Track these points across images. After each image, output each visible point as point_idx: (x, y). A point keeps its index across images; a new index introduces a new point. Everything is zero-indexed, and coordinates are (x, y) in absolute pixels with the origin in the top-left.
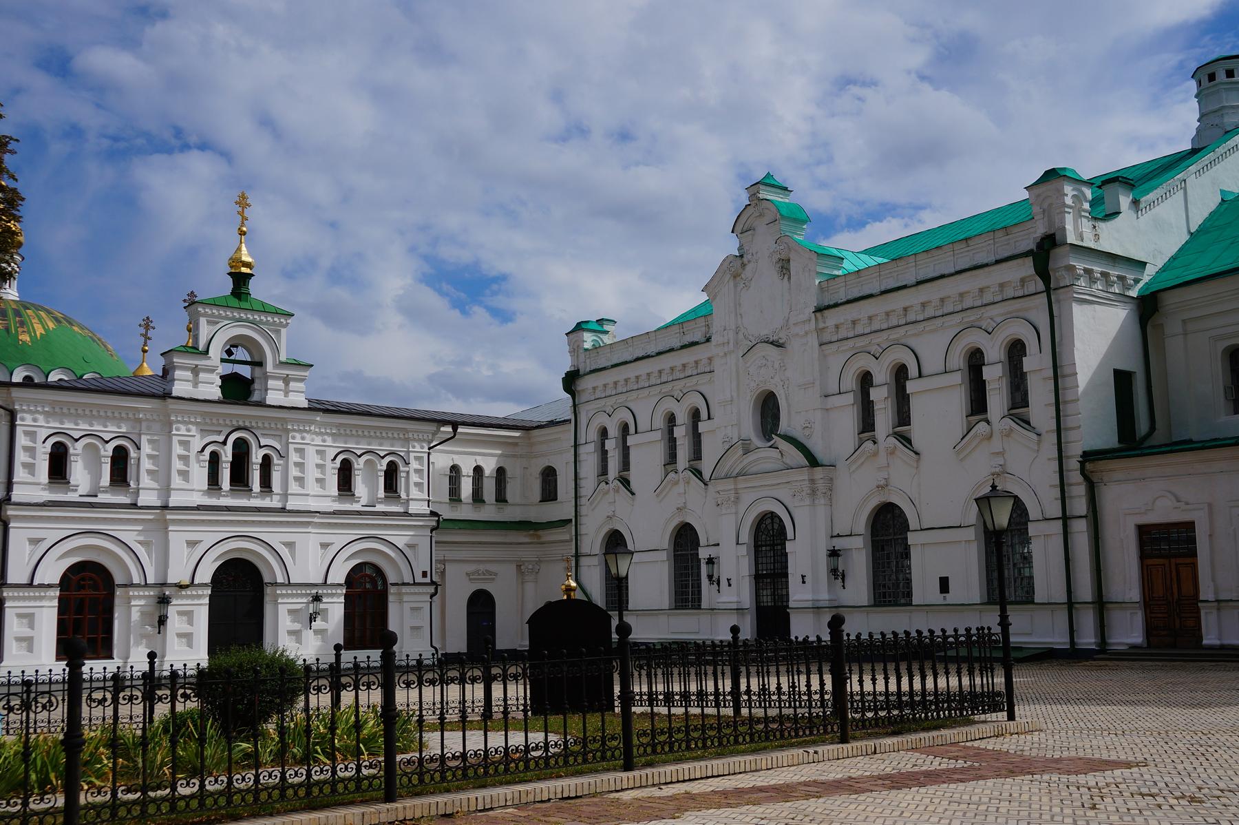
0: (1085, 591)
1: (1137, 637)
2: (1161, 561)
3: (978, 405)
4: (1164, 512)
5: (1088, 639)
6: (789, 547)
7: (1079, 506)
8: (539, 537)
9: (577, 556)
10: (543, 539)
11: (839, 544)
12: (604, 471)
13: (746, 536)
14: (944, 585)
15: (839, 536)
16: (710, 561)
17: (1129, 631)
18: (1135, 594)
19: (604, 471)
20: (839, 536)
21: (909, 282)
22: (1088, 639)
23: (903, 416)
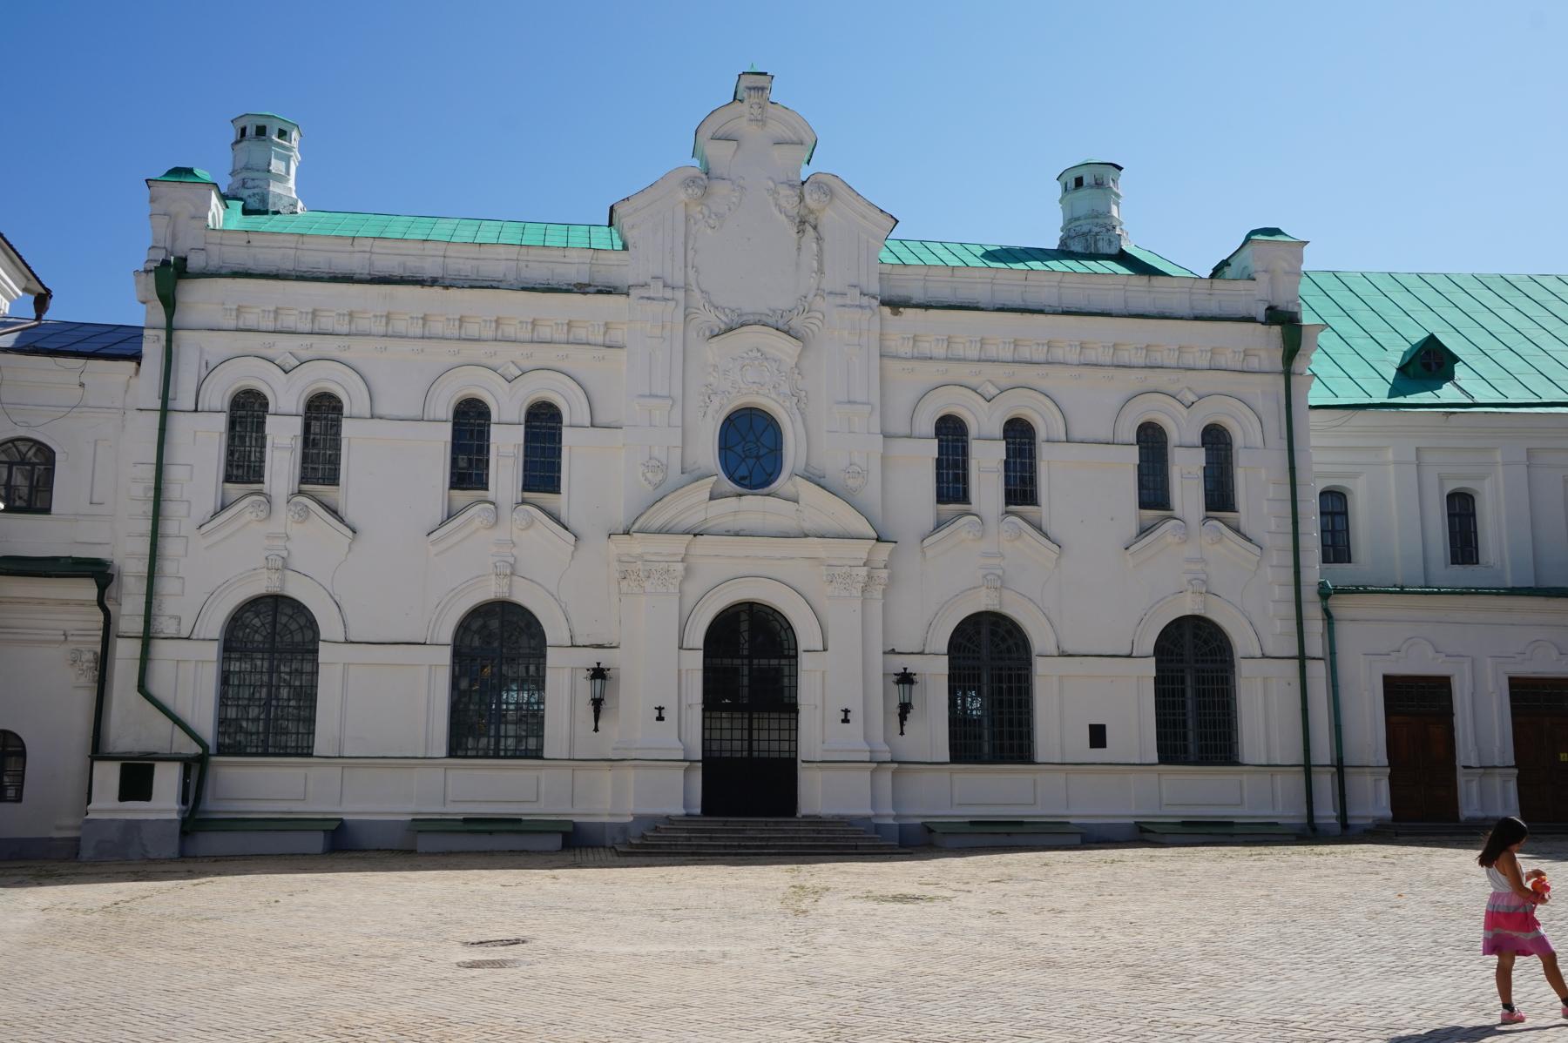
0: (1323, 752)
3: (1154, 493)
6: (806, 662)
7: (1315, 646)
11: (913, 664)
13: (697, 637)
14: (1098, 736)
16: (598, 673)
22: (1326, 812)
23: (1021, 488)
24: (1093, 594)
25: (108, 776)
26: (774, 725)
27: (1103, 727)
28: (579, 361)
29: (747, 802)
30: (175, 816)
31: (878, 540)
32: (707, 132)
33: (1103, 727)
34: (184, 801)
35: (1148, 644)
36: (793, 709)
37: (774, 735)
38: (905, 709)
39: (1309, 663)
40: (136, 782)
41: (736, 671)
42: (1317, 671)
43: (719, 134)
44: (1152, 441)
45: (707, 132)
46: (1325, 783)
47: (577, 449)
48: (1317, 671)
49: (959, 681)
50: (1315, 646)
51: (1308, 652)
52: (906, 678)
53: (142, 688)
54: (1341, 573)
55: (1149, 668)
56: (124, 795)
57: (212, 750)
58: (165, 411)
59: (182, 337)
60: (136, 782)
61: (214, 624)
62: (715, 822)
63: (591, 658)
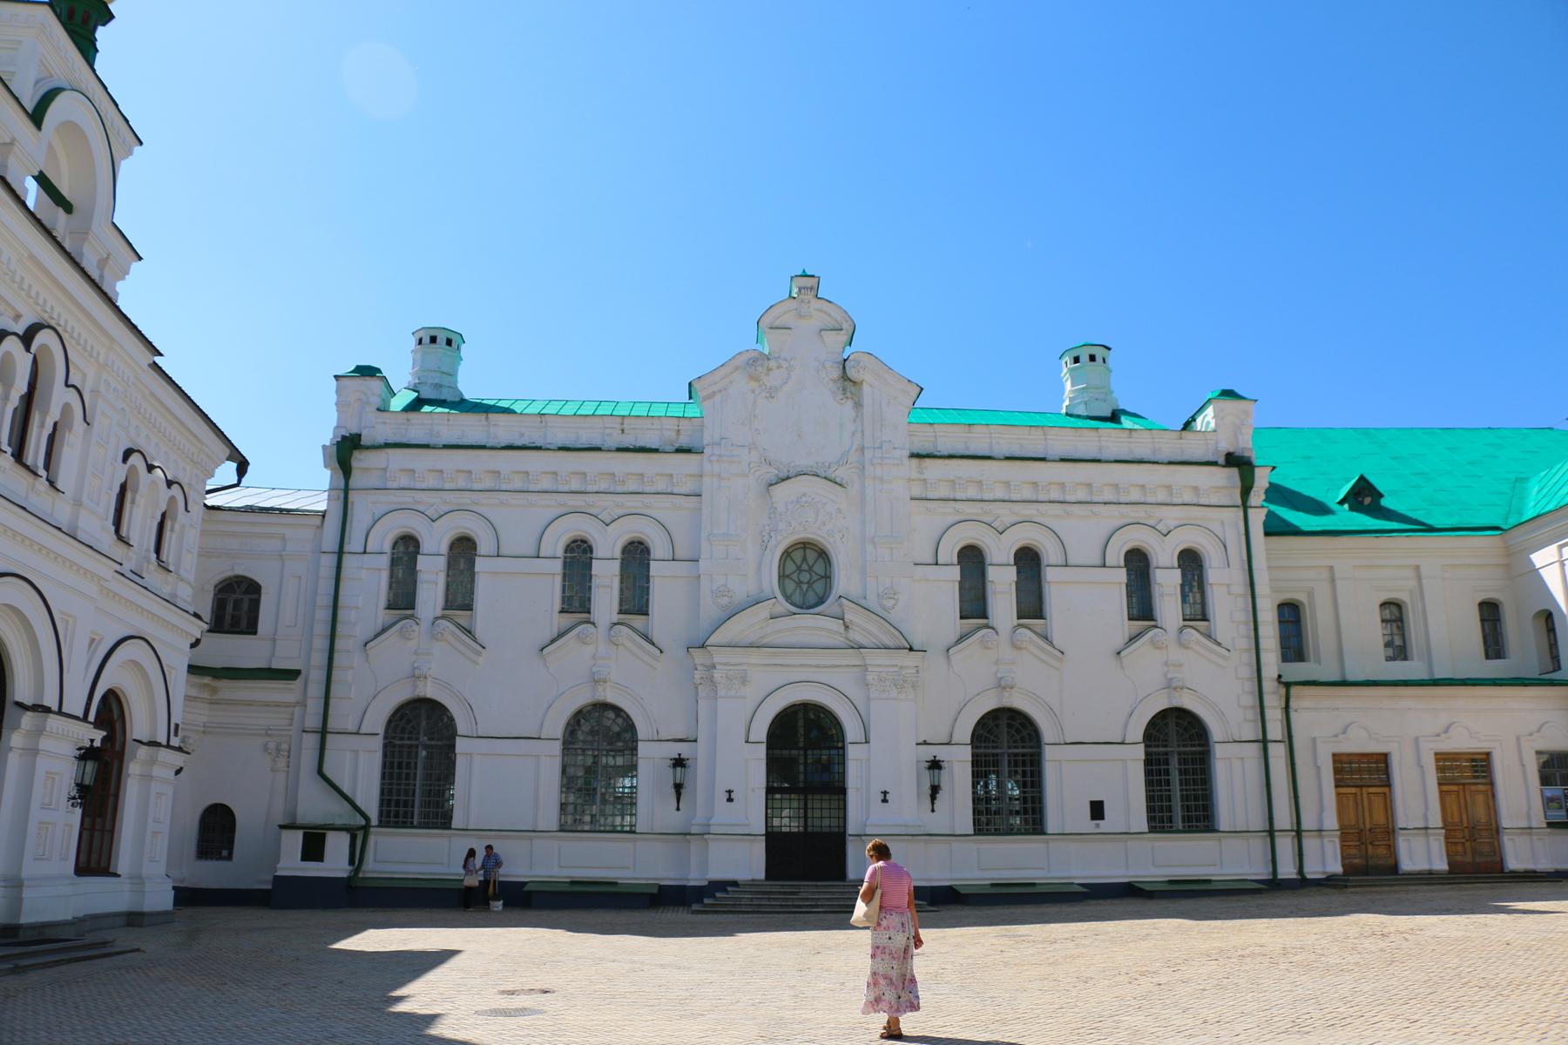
0: (1283, 819)
1: (1336, 867)
2: (1353, 790)
4: (1359, 743)
5: (1287, 870)
6: (853, 753)
7: (1275, 730)
8: (214, 690)
9: (323, 732)
10: (221, 695)
11: (941, 753)
12: (402, 598)
13: (761, 731)
14: (1097, 810)
15: (925, 743)
16: (679, 762)
17: (1325, 859)
18: (1331, 822)
19: (402, 598)
20: (925, 743)
21: (1050, 454)
23: (1032, 606)
24: (1092, 690)
25: (293, 842)
26: (825, 805)
27: (1101, 803)
28: (661, 508)
29: (805, 874)
30: (345, 875)
31: (911, 649)
32: (766, 321)
33: (1101, 803)
34: (351, 862)
35: (1137, 732)
36: (842, 791)
37: (826, 813)
38: (935, 790)
39: (1271, 746)
40: (314, 847)
41: (794, 760)
42: (1278, 753)
43: (776, 324)
44: (1138, 563)
45: (766, 321)
46: (1285, 846)
47: (663, 579)
48: (1278, 753)
49: (981, 767)
50: (1275, 730)
51: (1270, 736)
52: (935, 765)
53: (320, 772)
54: (1296, 671)
55: (1140, 752)
56: (305, 857)
57: (374, 821)
58: (340, 553)
59: (353, 496)
60: (314, 847)
61: (377, 721)
62: (776, 886)
63: (675, 750)
